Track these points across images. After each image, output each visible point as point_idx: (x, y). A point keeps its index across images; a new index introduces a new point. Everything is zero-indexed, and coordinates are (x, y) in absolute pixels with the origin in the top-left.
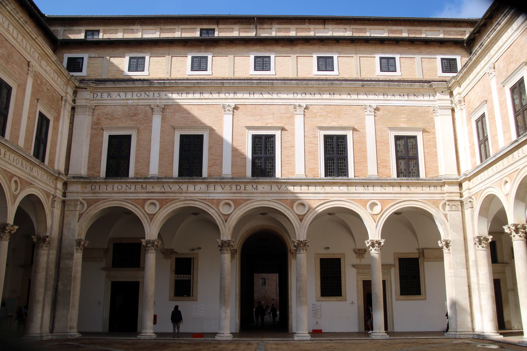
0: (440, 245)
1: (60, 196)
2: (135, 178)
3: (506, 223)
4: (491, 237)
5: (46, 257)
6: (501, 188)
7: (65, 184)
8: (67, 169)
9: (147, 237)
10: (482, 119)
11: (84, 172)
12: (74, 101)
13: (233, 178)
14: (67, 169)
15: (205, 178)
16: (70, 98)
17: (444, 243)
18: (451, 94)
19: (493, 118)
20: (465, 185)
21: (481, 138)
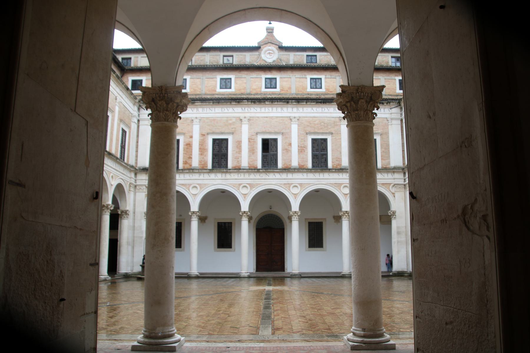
0: (389, 214)
5: (125, 224)
7: (136, 174)
9: (192, 210)
12: (139, 115)
13: (250, 169)
14: (136, 163)
15: (230, 169)
16: (136, 113)
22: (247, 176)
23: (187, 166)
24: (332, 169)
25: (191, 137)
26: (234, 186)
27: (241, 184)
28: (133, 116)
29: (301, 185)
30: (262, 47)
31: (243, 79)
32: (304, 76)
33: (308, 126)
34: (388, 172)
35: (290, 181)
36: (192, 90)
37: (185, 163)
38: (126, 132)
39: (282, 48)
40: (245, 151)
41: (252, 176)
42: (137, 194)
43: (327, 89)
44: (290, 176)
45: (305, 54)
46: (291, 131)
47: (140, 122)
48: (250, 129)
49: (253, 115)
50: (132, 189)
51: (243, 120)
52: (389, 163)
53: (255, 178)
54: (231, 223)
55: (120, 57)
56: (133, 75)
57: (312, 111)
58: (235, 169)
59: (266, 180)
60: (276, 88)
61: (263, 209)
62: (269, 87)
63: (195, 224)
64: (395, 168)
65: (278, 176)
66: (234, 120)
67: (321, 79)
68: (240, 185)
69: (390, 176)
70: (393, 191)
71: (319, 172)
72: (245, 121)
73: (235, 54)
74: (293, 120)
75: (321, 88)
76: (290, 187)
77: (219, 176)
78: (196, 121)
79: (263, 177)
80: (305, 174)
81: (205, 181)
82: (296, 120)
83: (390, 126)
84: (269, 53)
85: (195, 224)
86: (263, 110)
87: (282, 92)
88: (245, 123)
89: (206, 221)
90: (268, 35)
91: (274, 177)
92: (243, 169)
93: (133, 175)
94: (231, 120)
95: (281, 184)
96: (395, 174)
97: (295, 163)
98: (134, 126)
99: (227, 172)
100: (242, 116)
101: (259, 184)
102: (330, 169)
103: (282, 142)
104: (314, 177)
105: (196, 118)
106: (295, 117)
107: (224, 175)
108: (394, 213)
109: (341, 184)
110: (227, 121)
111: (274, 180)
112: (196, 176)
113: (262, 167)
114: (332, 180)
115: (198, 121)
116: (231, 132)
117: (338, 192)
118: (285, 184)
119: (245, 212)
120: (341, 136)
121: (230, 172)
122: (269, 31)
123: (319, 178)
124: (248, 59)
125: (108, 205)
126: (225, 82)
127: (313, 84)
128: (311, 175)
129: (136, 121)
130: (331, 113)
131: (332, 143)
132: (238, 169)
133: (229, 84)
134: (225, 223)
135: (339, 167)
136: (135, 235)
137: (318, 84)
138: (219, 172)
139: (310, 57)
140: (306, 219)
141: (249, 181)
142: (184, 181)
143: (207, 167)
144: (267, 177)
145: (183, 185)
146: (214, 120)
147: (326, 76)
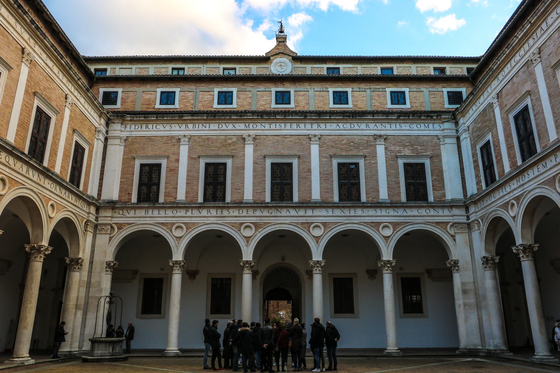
1: (93, 221)
2: (163, 203)
3: (514, 243)
4: (498, 257)
5: (77, 278)
6: (508, 211)
7: (98, 210)
8: (99, 194)
10: (487, 146)
11: (115, 196)
14: (99, 194)
15: (228, 203)
16: (104, 130)
17: (452, 263)
18: (457, 123)
19: (497, 146)
20: (472, 209)
21: (486, 164)
22: (251, 212)
23: (169, 199)
24: (366, 203)
25: (178, 160)
26: (233, 225)
27: (244, 223)
28: (97, 131)
29: (324, 224)
30: (271, 58)
31: (248, 93)
32: (325, 89)
33: (332, 146)
34: (443, 207)
35: (310, 220)
36: (182, 106)
37: (167, 195)
38: (83, 150)
39: (297, 59)
40: (248, 179)
41: (258, 213)
42: (98, 236)
43: (354, 105)
44: (309, 212)
45: (325, 66)
46: (310, 154)
47: (110, 142)
48: (255, 151)
49: (259, 132)
50: (90, 229)
51: (247, 139)
52: (444, 195)
53: (262, 214)
54: (230, 279)
55: (92, 68)
56: (106, 86)
57: (338, 128)
58: (235, 203)
59: (277, 218)
60: (289, 103)
61: (272, 260)
62: (281, 102)
63: (177, 279)
64: (452, 200)
65: (293, 212)
66: (234, 139)
67: (347, 92)
68: (241, 224)
69: (446, 212)
70: (452, 232)
71: (349, 207)
72: (249, 141)
73: (237, 66)
74: (313, 139)
75: (347, 103)
76: (309, 227)
77: (213, 212)
78: (184, 141)
79: (273, 214)
80: (330, 211)
81: (193, 219)
82: (317, 139)
83: (441, 146)
84: (281, 66)
85: (177, 279)
86: (273, 126)
87: (298, 109)
88: (249, 142)
89: (197, 277)
90: (278, 45)
91: (288, 214)
92: (246, 203)
93: (93, 210)
94: (230, 139)
95: (297, 223)
96: (454, 209)
97: (316, 195)
98: (98, 146)
99: (222, 208)
100: (245, 133)
101: (268, 223)
102: (364, 203)
103: (299, 168)
104: (343, 214)
105: (185, 136)
106: (315, 136)
107: (219, 211)
108: (456, 263)
109: (380, 223)
110: (225, 140)
111: (288, 218)
112: (182, 213)
113: (272, 200)
114: (367, 218)
115: (186, 140)
116: (229, 154)
117: (375, 235)
118: (303, 223)
119: (247, 261)
120: (376, 160)
121: (228, 208)
122: (280, 40)
123: (349, 214)
124: (254, 70)
125: (41, 246)
126: (225, 96)
127: (337, 98)
128: (338, 212)
129: (103, 139)
130: (362, 130)
131: (365, 169)
132: (240, 205)
133: (229, 99)
134: (222, 280)
135: (375, 200)
136: (90, 295)
137: (343, 98)
138: (213, 207)
139: (331, 71)
140: (330, 274)
141: (254, 220)
142: (164, 219)
143: (197, 200)
144: (279, 214)
145: (163, 224)
146: (208, 139)
147: (353, 88)
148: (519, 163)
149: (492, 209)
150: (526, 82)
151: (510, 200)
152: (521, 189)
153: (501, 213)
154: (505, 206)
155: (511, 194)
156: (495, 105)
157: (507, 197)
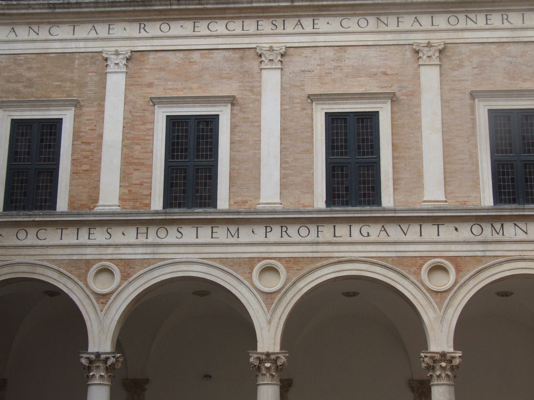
148: (157, 203)
149: (18, 259)
150: (230, 79)
151: (101, 260)
152: (149, 250)
153: (55, 275)
154: (80, 268)
155: (110, 250)
156: (112, 68)
157: (89, 250)
